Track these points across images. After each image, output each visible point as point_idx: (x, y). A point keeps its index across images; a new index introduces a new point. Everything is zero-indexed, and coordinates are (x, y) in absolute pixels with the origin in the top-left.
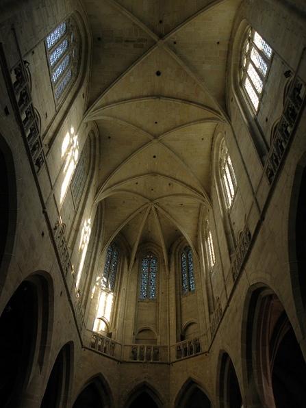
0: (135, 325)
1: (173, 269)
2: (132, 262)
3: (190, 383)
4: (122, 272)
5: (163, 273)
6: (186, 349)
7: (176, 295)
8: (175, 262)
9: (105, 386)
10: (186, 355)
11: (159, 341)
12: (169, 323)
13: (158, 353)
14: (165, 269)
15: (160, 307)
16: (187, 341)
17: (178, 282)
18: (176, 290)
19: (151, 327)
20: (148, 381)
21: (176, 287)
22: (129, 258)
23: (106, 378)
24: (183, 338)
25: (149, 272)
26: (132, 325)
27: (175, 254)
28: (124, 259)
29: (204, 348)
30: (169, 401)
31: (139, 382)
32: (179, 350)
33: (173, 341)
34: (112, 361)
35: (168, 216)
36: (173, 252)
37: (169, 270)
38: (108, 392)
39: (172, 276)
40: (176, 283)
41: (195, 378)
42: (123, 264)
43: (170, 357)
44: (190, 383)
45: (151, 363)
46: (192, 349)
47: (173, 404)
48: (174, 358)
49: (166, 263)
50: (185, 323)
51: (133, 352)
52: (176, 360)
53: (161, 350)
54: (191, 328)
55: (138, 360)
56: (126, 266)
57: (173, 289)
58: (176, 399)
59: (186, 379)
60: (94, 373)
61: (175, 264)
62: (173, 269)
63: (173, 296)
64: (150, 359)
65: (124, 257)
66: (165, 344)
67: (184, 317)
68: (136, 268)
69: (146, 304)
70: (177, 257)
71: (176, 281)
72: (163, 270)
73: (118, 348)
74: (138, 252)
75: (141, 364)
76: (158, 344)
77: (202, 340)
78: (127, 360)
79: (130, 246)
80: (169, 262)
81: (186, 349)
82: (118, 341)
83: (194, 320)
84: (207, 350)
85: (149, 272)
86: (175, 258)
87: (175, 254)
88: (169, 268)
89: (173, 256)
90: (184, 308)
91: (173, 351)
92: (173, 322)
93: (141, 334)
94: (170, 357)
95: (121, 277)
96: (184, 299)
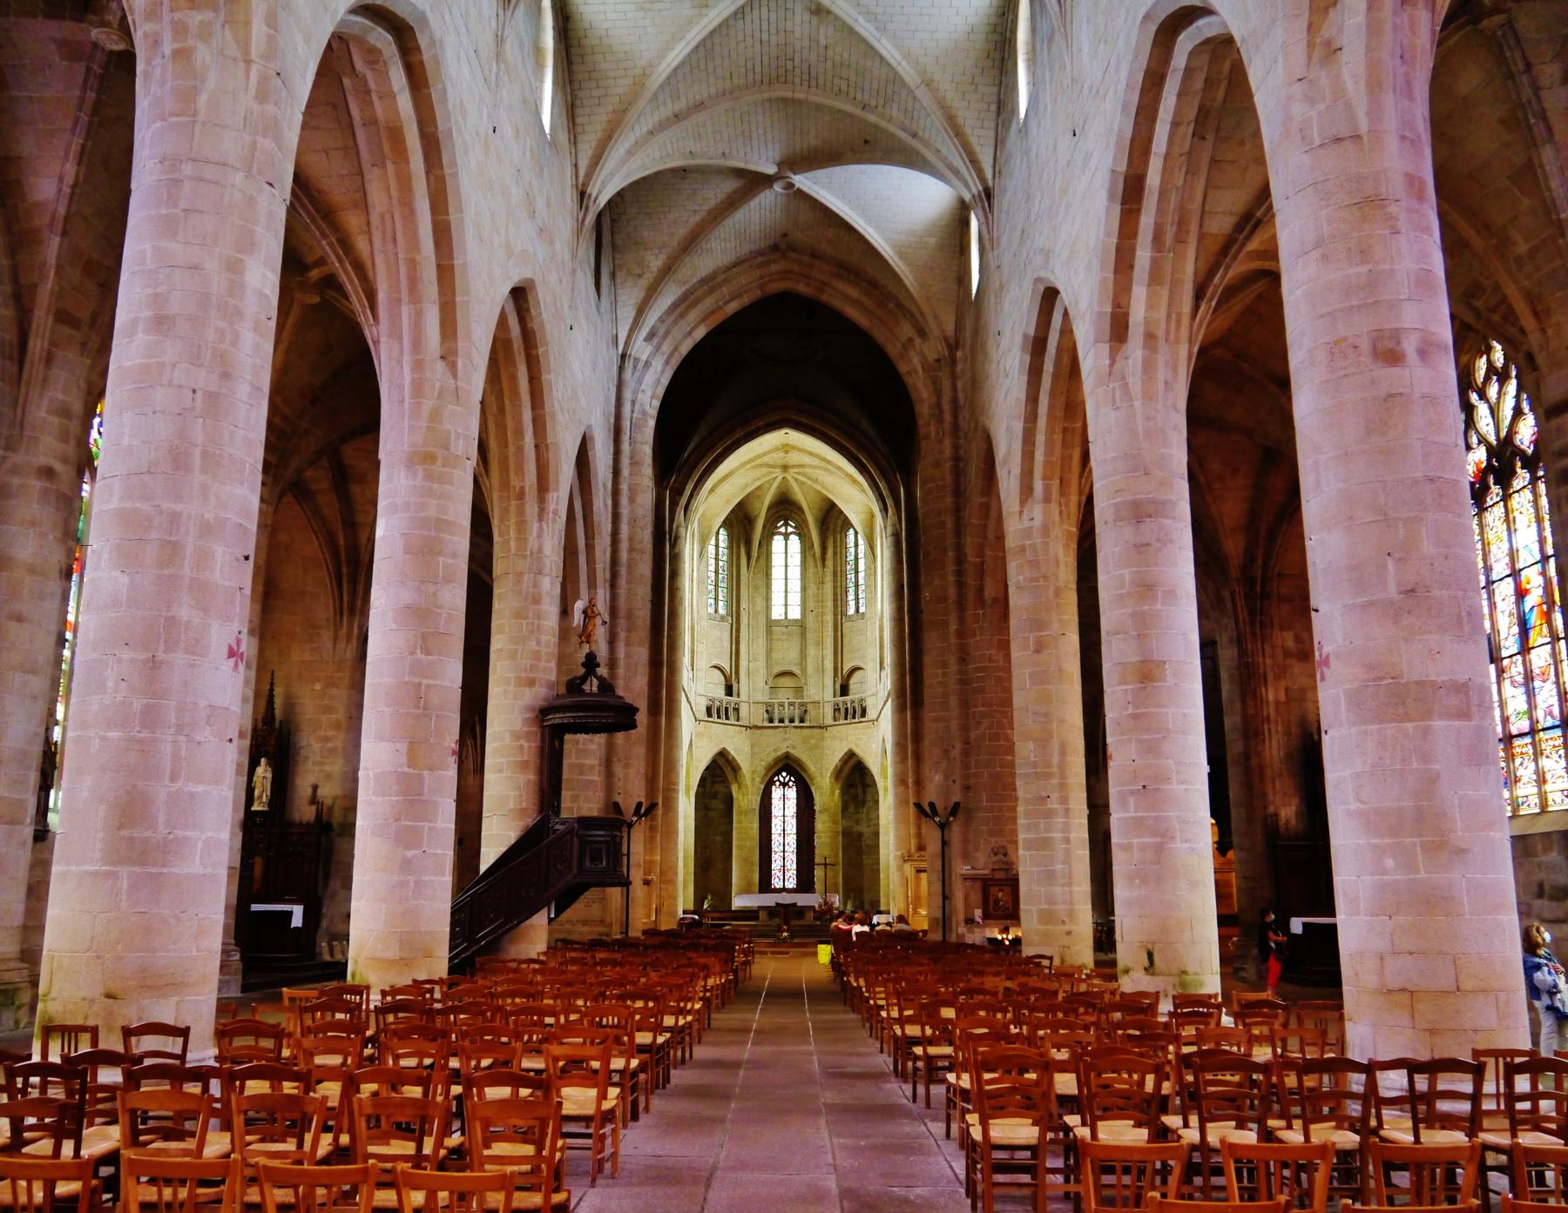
1: (829, 563)
2: (755, 554)
3: (851, 755)
6: (847, 709)
7: (835, 615)
8: (835, 547)
9: (735, 769)
10: (846, 718)
13: (806, 711)
19: (797, 672)
20: (791, 751)
24: (844, 690)
26: (763, 671)
28: (739, 547)
29: (871, 714)
31: (779, 753)
32: (837, 710)
35: (819, 488)
36: (832, 527)
37: (824, 565)
39: (829, 578)
41: (857, 750)
44: (851, 755)
46: (855, 712)
47: (827, 780)
48: (829, 720)
50: (847, 667)
52: (832, 722)
53: (810, 707)
54: (857, 675)
55: (776, 724)
60: (716, 750)
61: (835, 553)
66: (816, 699)
69: (784, 629)
71: (835, 588)
74: (764, 527)
77: (869, 703)
78: (760, 724)
80: (824, 548)
81: (847, 709)
83: (861, 665)
84: (875, 717)
86: (835, 542)
88: (824, 559)
91: (829, 711)
92: (829, 665)
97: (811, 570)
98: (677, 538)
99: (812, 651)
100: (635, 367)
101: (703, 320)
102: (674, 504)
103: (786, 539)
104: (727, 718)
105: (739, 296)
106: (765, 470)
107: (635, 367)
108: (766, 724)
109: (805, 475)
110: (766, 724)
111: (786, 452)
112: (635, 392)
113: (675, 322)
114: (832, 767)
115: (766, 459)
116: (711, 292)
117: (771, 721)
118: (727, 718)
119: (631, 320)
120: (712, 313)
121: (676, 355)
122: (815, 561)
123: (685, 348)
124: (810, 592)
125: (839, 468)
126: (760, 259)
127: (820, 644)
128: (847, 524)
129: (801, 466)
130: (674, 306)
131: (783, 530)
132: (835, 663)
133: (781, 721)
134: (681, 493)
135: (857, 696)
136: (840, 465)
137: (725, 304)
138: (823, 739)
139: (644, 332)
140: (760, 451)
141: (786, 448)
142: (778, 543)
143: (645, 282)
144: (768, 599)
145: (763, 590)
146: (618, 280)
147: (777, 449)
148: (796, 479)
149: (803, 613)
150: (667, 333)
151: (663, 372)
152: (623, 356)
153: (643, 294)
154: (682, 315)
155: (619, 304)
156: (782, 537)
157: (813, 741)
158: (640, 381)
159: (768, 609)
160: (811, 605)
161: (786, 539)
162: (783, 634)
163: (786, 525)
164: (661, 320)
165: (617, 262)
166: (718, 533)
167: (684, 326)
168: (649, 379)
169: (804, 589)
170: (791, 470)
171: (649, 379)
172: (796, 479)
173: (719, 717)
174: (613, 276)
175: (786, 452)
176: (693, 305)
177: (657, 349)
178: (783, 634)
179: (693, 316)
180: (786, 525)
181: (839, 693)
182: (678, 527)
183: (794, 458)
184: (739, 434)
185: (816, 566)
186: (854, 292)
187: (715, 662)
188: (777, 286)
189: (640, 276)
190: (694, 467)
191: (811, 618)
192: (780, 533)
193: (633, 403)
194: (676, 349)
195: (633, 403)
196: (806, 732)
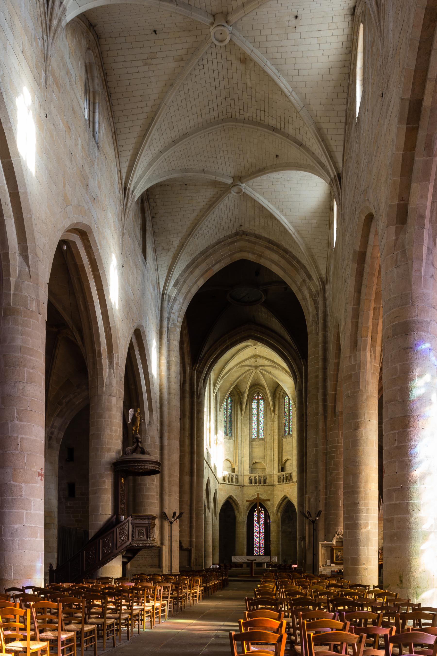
0: (249, 460)
1: (277, 412)
2: (244, 409)
3: (285, 498)
4: (237, 419)
5: (269, 416)
6: (284, 477)
7: (279, 436)
8: (279, 405)
10: (283, 482)
11: (266, 470)
12: (274, 459)
14: (271, 412)
15: (267, 445)
16: (284, 473)
17: (281, 425)
18: (279, 432)
21: (279, 429)
22: (241, 404)
23: (235, 497)
25: (258, 414)
27: (279, 398)
28: (237, 406)
30: (273, 506)
32: (279, 478)
33: (276, 472)
34: (237, 486)
38: (237, 504)
39: (276, 420)
40: (279, 426)
42: (237, 411)
43: (274, 481)
44: (285, 498)
45: (262, 486)
48: (276, 482)
49: (272, 408)
50: (284, 459)
51: (249, 479)
53: (268, 477)
56: (239, 412)
57: (277, 431)
58: (277, 506)
59: (283, 496)
60: (227, 496)
61: (279, 408)
62: (277, 412)
63: (276, 437)
64: (261, 483)
65: (237, 404)
66: (271, 473)
67: (284, 454)
68: (247, 412)
69: (257, 443)
70: (281, 400)
71: (279, 423)
72: (269, 413)
73: (240, 478)
74: (248, 396)
75: (256, 487)
76: (266, 473)
79: (241, 392)
80: (274, 405)
81: (284, 477)
82: (240, 474)
85: (258, 414)
86: (279, 403)
87: (279, 398)
88: (274, 411)
89: (277, 399)
90: (284, 447)
91: (276, 479)
92: (276, 458)
93: (254, 465)
94: (274, 481)
95: (237, 423)
96: (284, 440)
97: (269, 416)
98: (200, 394)
99: (269, 452)
100: (169, 301)
101: (202, 275)
102: (198, 378)
103: (258, 400)
104: (232, 482)
105: (220, 261)
106: (247, 368)
107: (169, 301)
108: (248, 485)
109: (265, 370)
110: (248, 485)
111: (256, 359)
112: (170, 314)
113: (188, 276)
114: (278, 503)
115: (247, 363)
116: (205, 259)
117: (251, 483)
118: (232, 482)
119: (166, 275)
120: (207, 271)
121: (189, 294)
122: (271, 412)
123: (194, 290)
124: (268, 426)
125: (280, 366)
126: (229, 240)
127: (272, 449)
128: (285, 394)
129: (263, 366)
130: (188, 267)
131: (257, 398)
132: (279, 457)
133: (256, 483)
134: (200, 372)
135: (289, 472)
136: (280, 363)
137: (213, 266)
138: (273, 491)
139: (172, 282)
140: (244, 358)
141: (256, 356)
142: (254, 403)
143: (171, 254)
144: (250, 429)
145: (248, 426)
146: (158, 253)
147: (251, 357)
148: (261, 373)
149: (265, 436)
150: (185, 282)
151: (183, 303)
152: (163, 295)
153: (171, 260)
154: (191, 273)
155: (159, 266)
156: (256, 401)
157: (269, 492)
158: (172, 308)
159: (250, 434)
160: (269, 432)
161: (258, 400)
162: (257, 445)
163: (258, 395)
164: (181, 275)
165: (156, 242)
166: (227, 400)
167: (193, 278)
168: (176, 307)
169: (266, 425)
170: (259, 368)
171: (176, 307)
172: (261, 373)
173: (229, 482)
174: (155, 249)
175: (256, 359)
176: (197, 267)
177: (179, 291)
178: (257, 445)
179: (197, 272)
180: (258, 395)
181: (281, 470)
182: (200, 389)
183: (261, 362)
184: (228, 343)
185: (271, 414)
186: (275, 257)
187: (227, 458)
188: (238, 256)
189: (169, 250)
190: (207, 360)
191: (268, 438)
192: (256, 399)
193: (169, 319)
194: (189, 291)
195: (169, 319)
196: (267, 488)
